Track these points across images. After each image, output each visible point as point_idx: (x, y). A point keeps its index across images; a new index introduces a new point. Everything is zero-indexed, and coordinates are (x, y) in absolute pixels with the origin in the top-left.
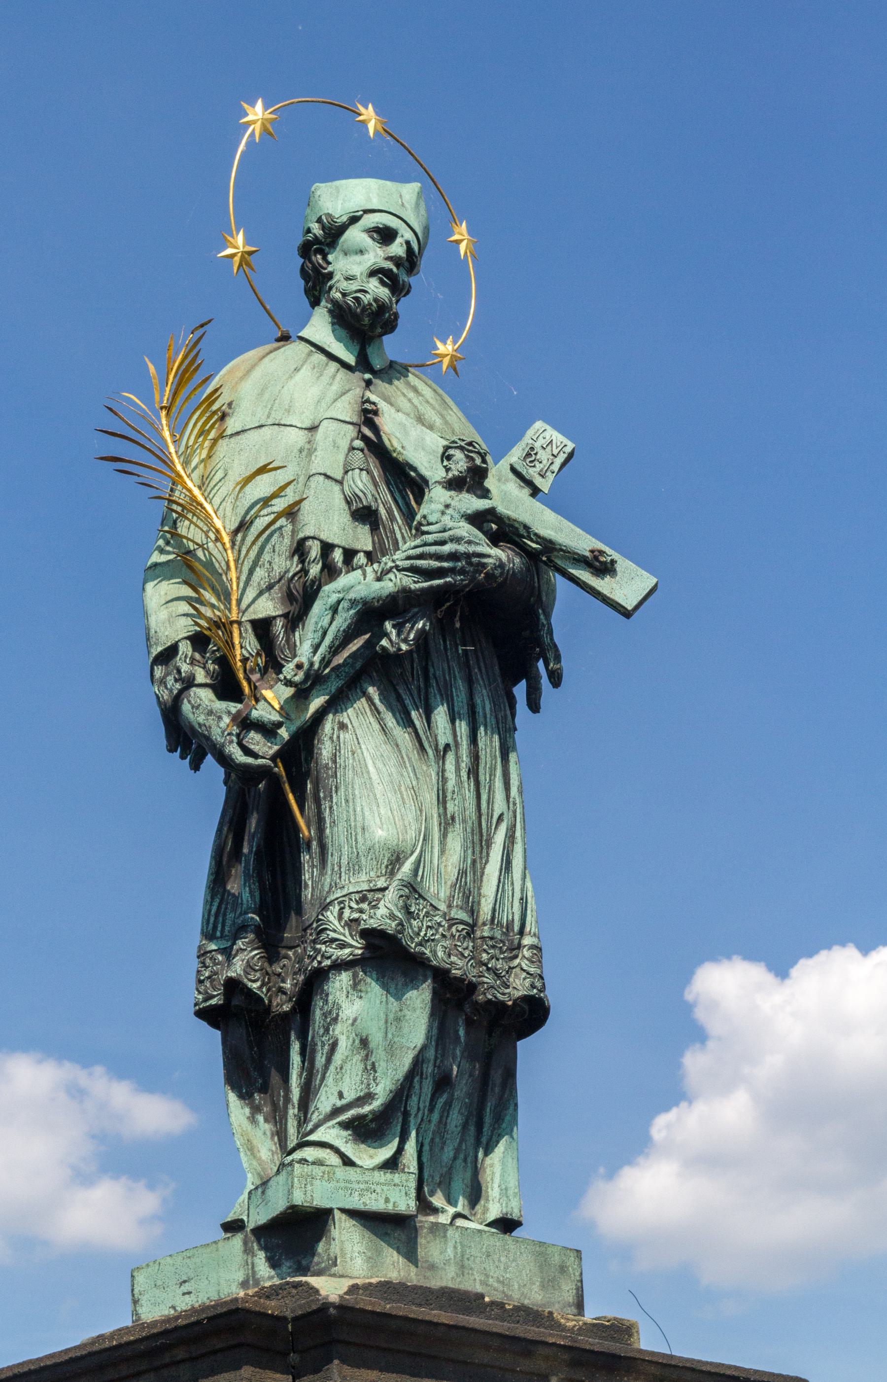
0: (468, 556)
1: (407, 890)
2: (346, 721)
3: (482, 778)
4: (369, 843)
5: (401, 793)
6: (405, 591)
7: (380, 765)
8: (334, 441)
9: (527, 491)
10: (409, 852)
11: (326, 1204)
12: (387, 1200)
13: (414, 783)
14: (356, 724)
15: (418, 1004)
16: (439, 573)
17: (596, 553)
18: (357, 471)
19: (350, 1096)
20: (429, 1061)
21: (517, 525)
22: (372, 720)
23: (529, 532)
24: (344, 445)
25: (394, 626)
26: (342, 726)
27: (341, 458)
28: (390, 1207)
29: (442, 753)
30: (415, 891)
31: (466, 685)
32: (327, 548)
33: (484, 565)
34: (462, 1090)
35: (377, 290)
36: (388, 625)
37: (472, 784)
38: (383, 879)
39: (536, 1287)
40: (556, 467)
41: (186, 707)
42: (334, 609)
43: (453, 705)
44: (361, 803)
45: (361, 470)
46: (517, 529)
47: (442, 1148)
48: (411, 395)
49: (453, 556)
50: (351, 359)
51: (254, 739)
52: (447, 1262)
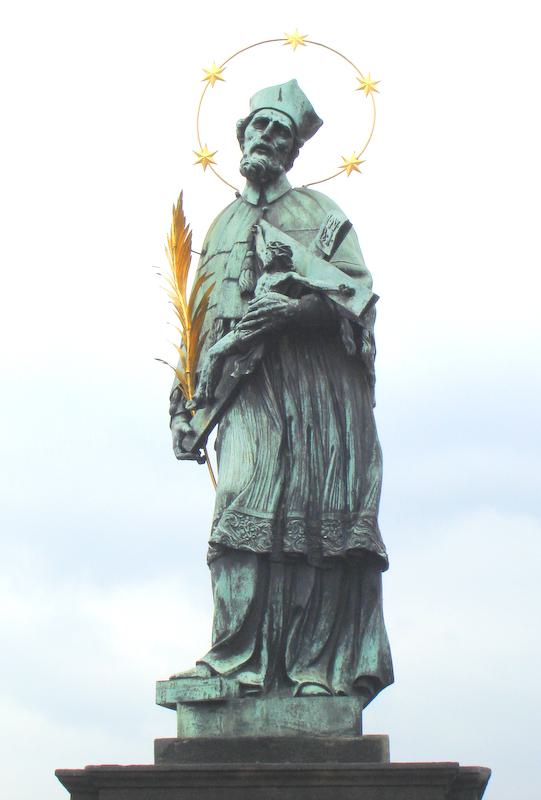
9: (321, 257)
11: (174, 701)
12: (205, 694)
13: (255, 447)
15: (250, 576)
19: (221, 632)
20: (277, 602)
24: (242, 256)
28: (207, 697)
30: (241, 514)
31: (310, 377)
32: (227, 321)
34: (327, 608)
35: (257, 158)
40: (333, 238)
47: (311, 645)
48: (294, 209)
49: (261, 314)
50: (255, 203)
52: (258, 719)
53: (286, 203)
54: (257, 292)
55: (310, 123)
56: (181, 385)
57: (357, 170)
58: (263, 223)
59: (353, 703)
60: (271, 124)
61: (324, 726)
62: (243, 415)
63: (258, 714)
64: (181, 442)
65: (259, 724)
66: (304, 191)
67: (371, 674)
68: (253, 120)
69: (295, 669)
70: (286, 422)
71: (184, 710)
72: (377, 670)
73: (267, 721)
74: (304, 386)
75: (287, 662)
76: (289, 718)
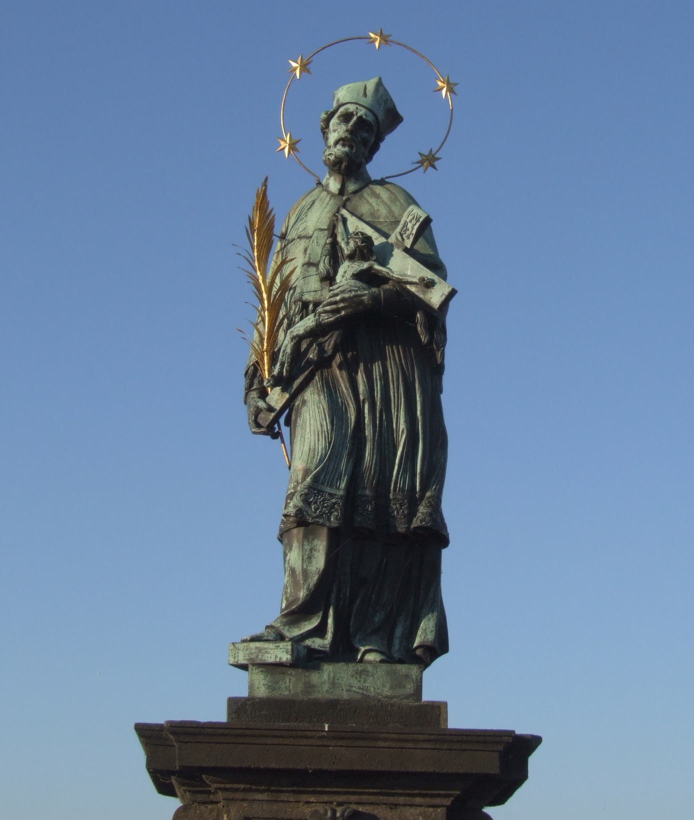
0: (349, 298)
12: (276, 657)
16: (337, 311)
24: (322, 242)
26: (304, 402)
28: (278, 660)
32: (305, 305)
33: (362, 301)
39: (386, 689)
40: (414, 232)
48: (372, 201)
49: (343, 300)
52: (324, 682)
53: (365, 195)
54: (338, 278)
55: (393, 118)
56: (257, 362)
57: (434, 167)
58: (344, 212)
59: (414, 670)
60: (355, 118)
61: (386, 691)
63: (325, 677)
64: (256, 417)
65: (326, 687)
66: (382, 182)
67: (429, 644)
69: (358, 637)
71: (256, 671)
72: (435, 640)
73: (333, 684)
75: (351, 630)
76: (355, 683)
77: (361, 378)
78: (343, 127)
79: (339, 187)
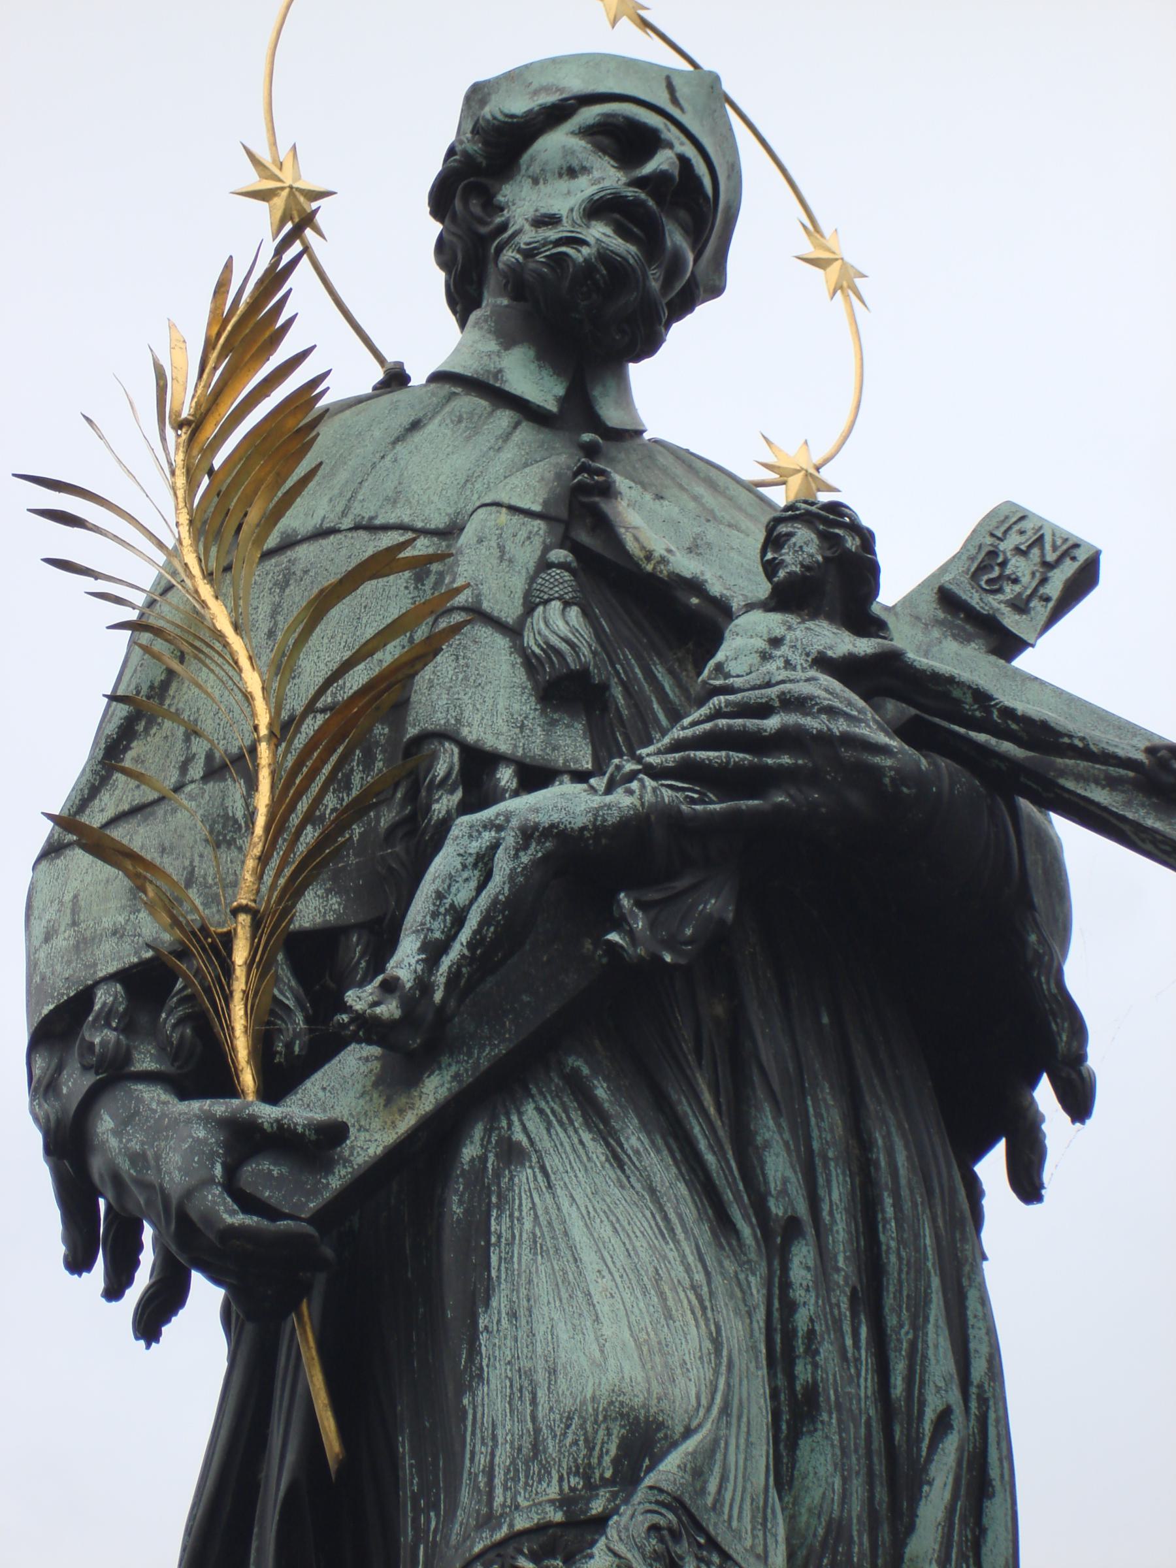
1: (671, 1516)
2: (519, 1136)
3: (892, 1321)
4: (568, 1403)
5: (662, 1295)
6: (670, 817)
7: (606, 1231)
8: (502, 549)
10: (679, 1429)
14: (544, 1143)
17: (1163, 753)
18: (556, 605)
21: (957, 693)
22: (586, 1137)
23: (987, 710)
24: (527, 555)
25: (640, 904)
26: (512, 1154)
27: (518, 584)
29: (779, 1238)
36: (625, 900)
37: (864, 1331)
38: (604, 1494)
40: (1054, 588)
41: (105, 1124)
42: (484, 863)
43: (808, 1139)
44: (549, 1314)
45: (567, 604)
46: (958, 702)
48: (700, 490)
51: (265, 1174)
62: (607, 1134)
64: (231, 1172)
68: (589, 114)
70: (779, 1238)
74: (828, 1123)
77: (769, 1129)
78: (607, 176)
79: (560, 390)
